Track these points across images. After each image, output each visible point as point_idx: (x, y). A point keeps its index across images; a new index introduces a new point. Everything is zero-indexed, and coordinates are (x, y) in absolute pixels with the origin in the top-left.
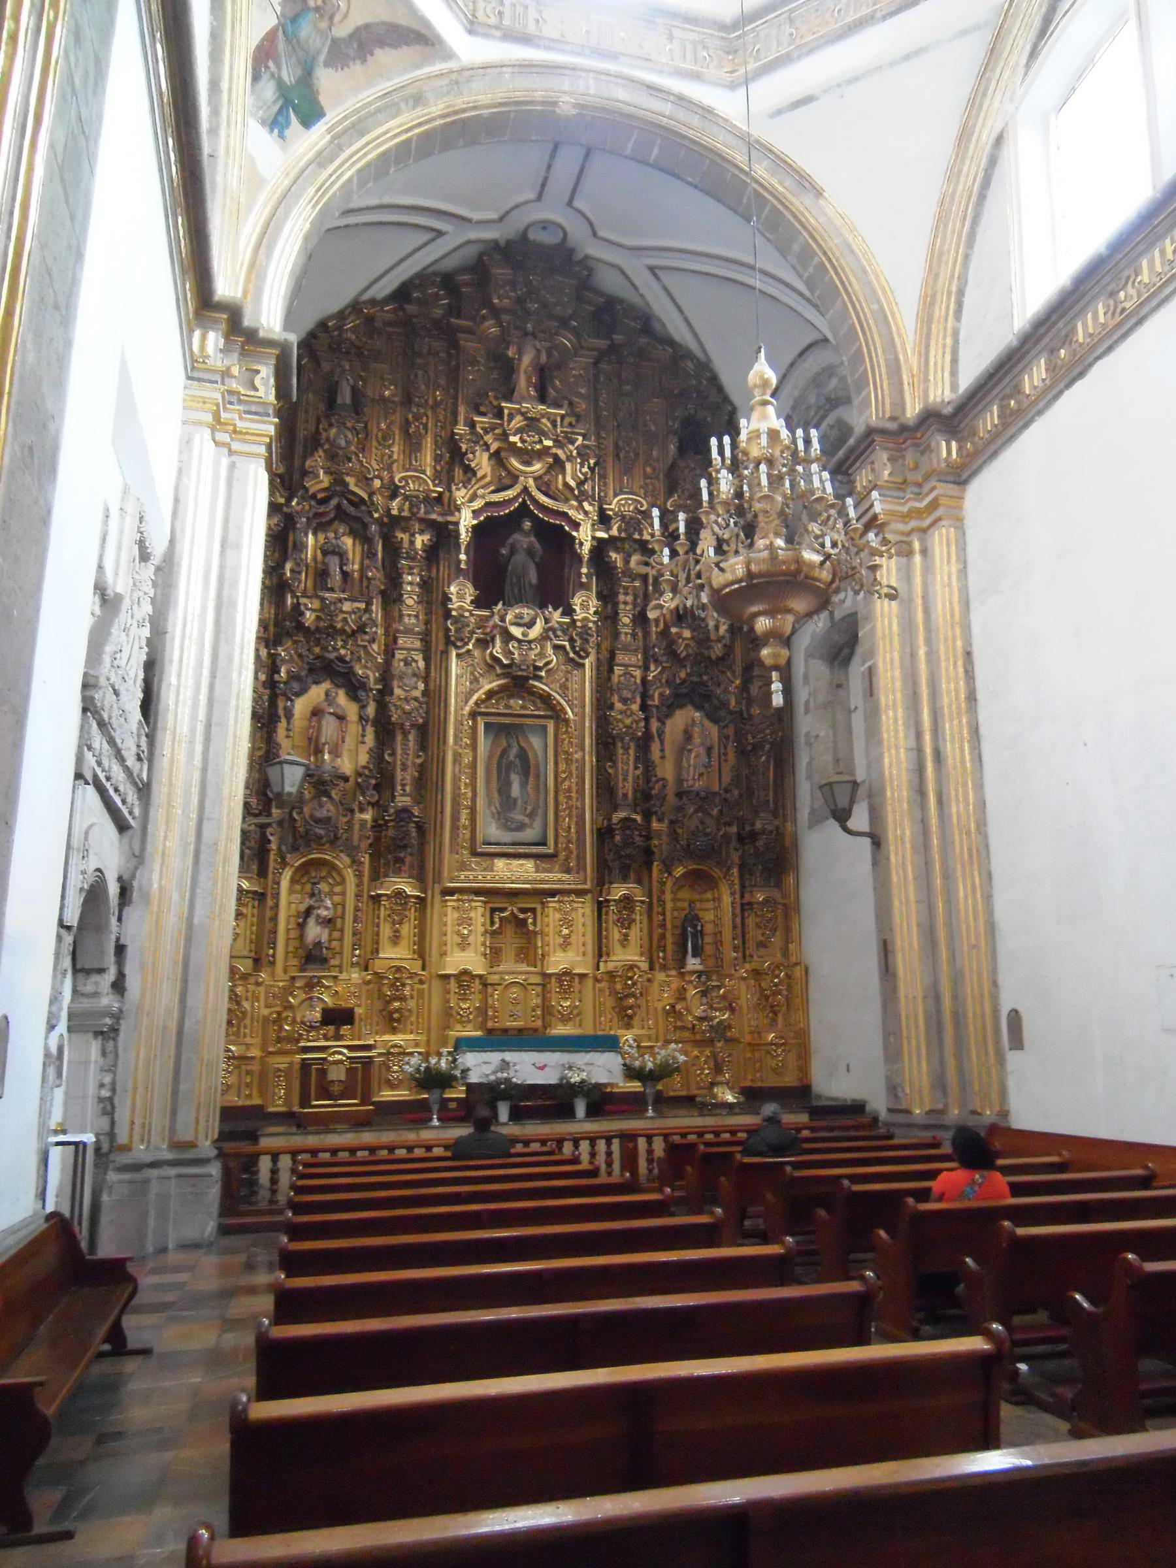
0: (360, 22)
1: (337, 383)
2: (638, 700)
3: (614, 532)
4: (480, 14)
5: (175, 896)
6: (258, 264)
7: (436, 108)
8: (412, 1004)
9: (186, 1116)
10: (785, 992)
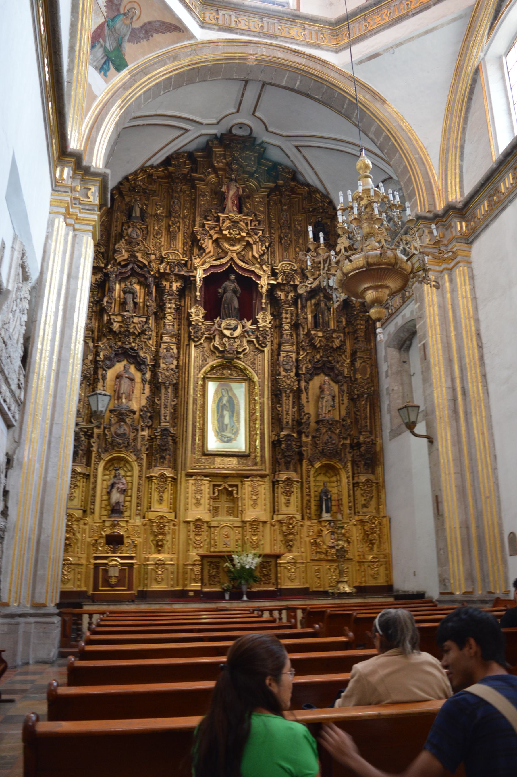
0: (146, 20)
1: (133, 206)
2: (294, 370)
3: (280, 280)
4: (207, 19)
5: (37, 465)
6: (91, 136)
7: (185, 61)
8: (169, 537)
9: (40, 589)
10: (378, 532)
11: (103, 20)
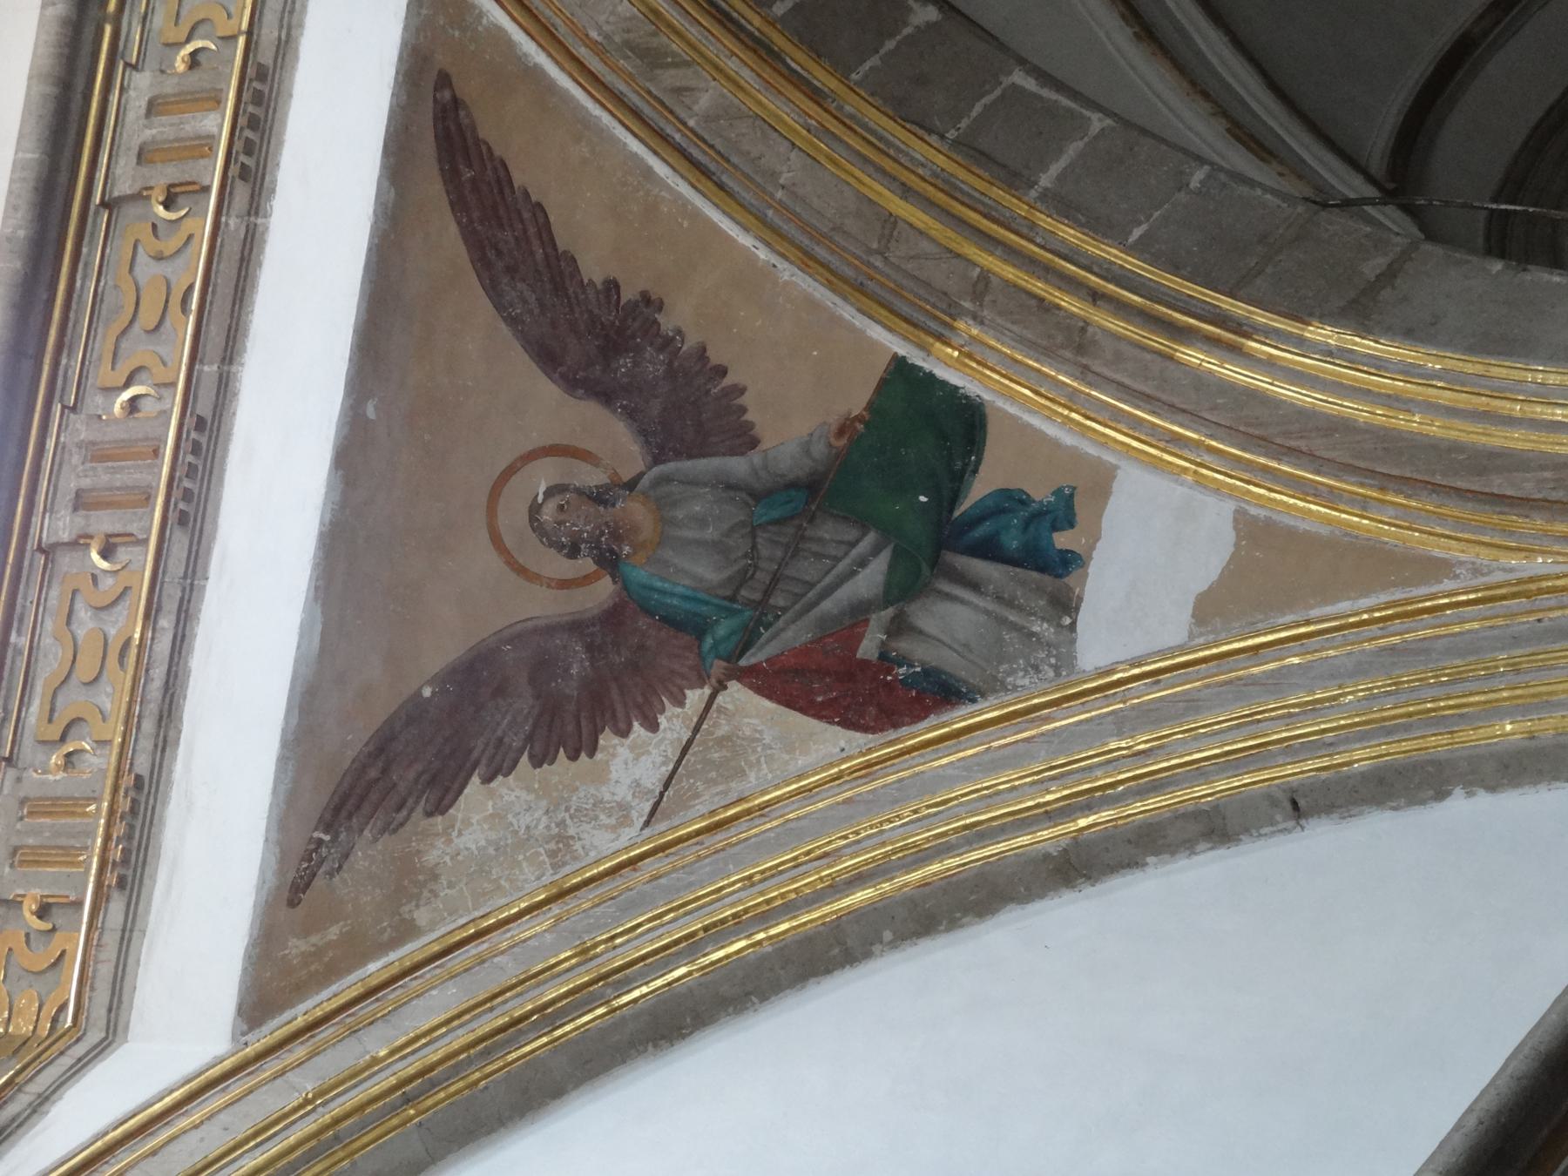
0: (547, 390)
11: (737, 694)
